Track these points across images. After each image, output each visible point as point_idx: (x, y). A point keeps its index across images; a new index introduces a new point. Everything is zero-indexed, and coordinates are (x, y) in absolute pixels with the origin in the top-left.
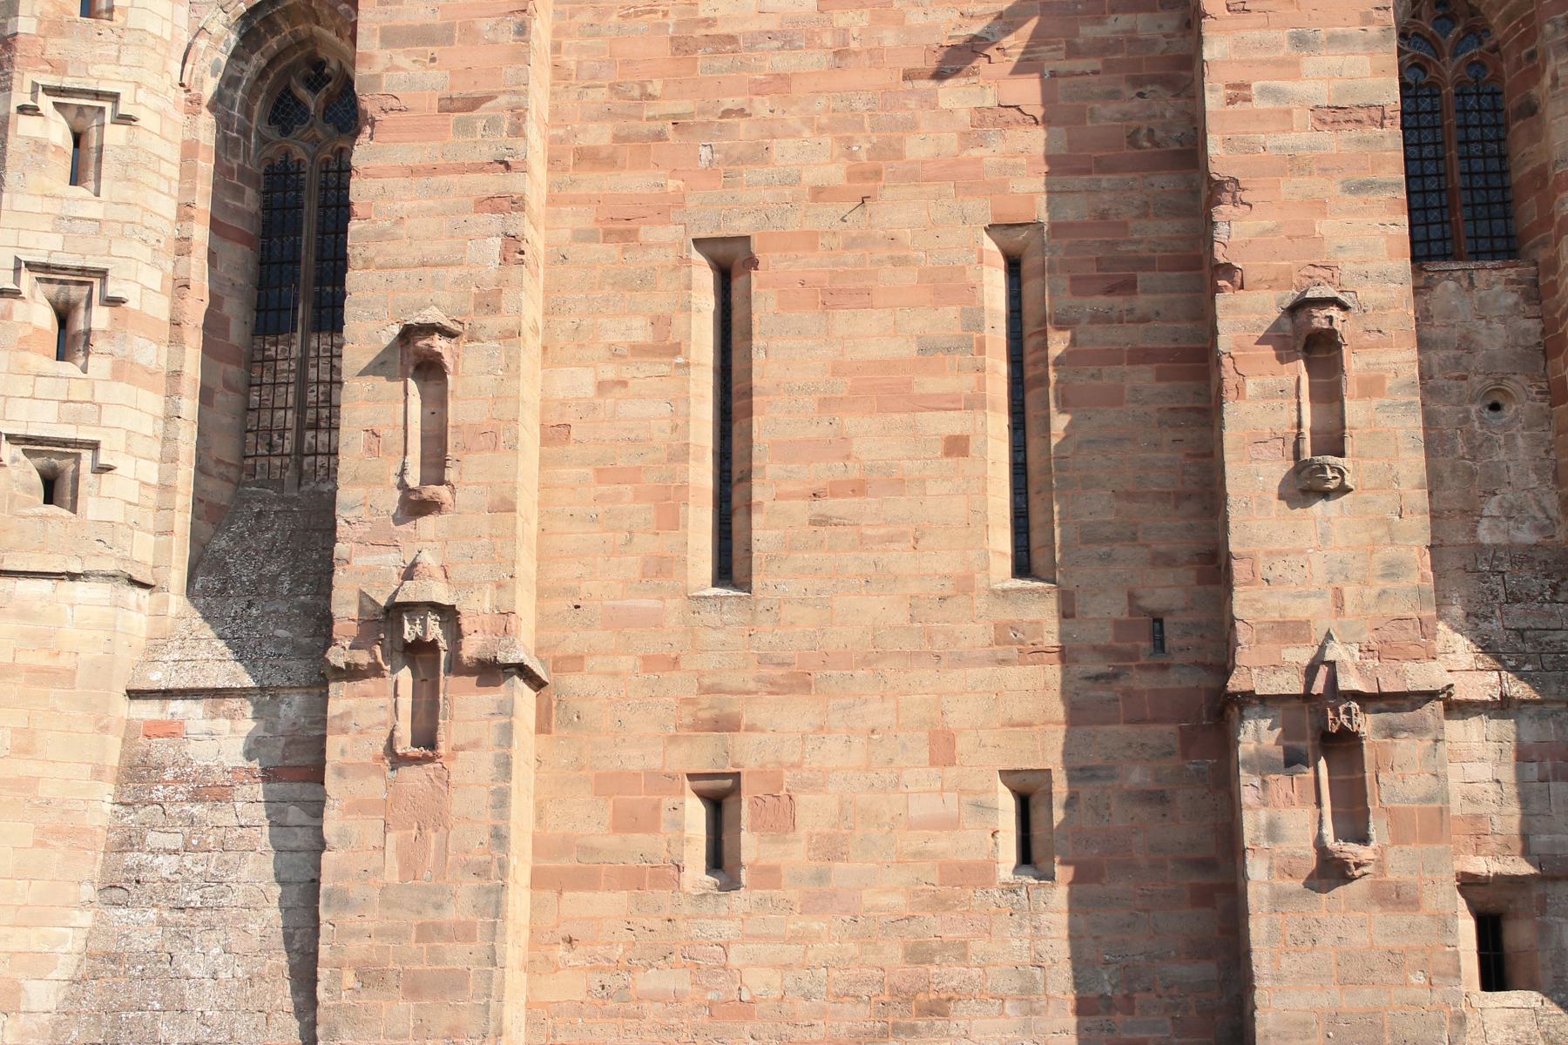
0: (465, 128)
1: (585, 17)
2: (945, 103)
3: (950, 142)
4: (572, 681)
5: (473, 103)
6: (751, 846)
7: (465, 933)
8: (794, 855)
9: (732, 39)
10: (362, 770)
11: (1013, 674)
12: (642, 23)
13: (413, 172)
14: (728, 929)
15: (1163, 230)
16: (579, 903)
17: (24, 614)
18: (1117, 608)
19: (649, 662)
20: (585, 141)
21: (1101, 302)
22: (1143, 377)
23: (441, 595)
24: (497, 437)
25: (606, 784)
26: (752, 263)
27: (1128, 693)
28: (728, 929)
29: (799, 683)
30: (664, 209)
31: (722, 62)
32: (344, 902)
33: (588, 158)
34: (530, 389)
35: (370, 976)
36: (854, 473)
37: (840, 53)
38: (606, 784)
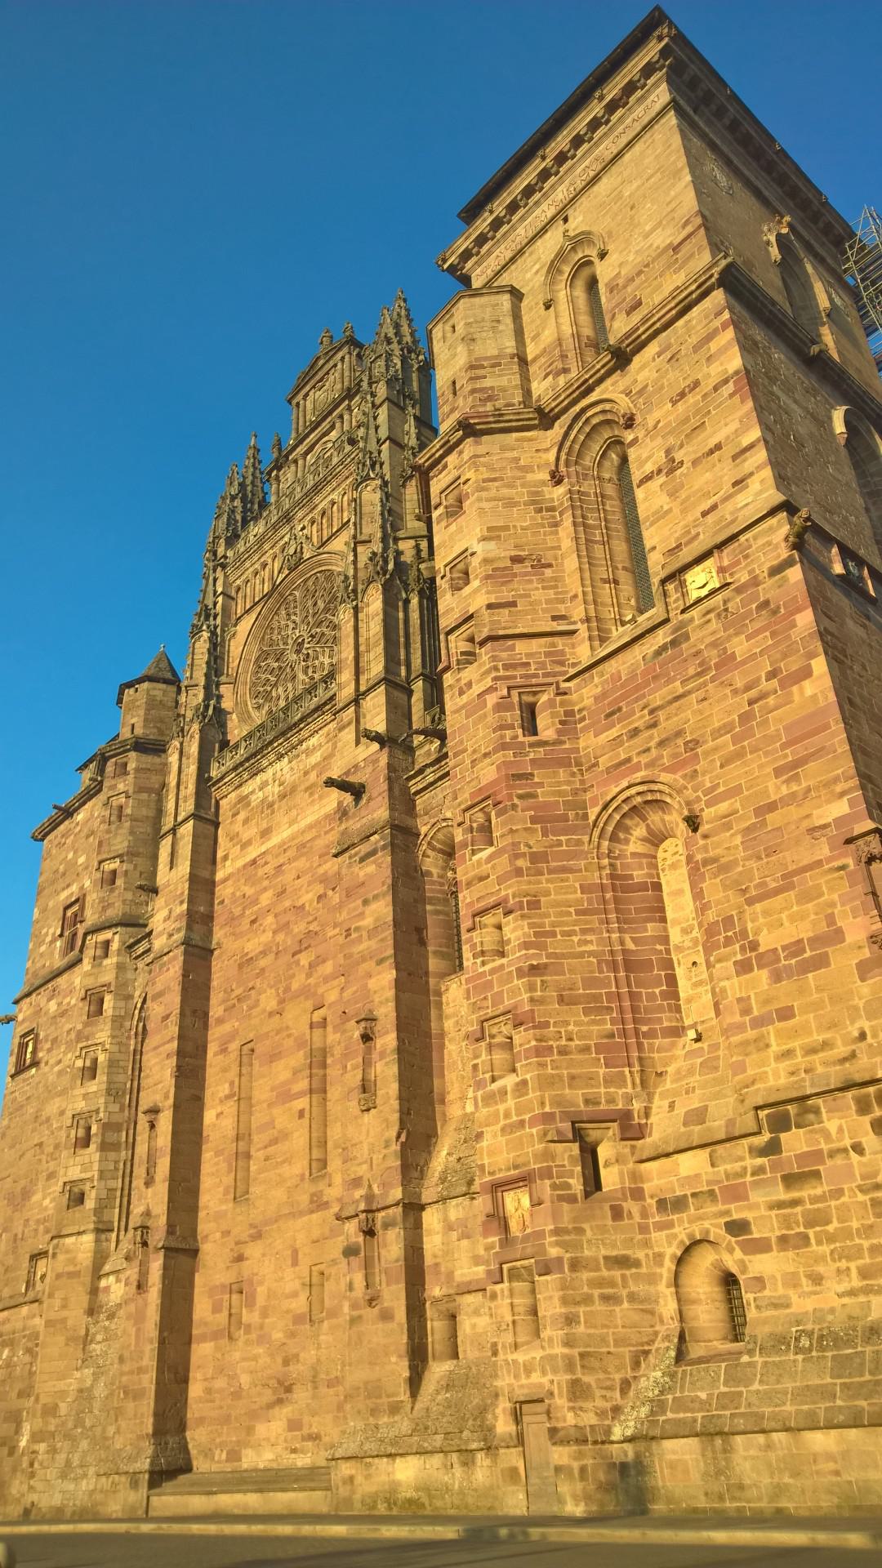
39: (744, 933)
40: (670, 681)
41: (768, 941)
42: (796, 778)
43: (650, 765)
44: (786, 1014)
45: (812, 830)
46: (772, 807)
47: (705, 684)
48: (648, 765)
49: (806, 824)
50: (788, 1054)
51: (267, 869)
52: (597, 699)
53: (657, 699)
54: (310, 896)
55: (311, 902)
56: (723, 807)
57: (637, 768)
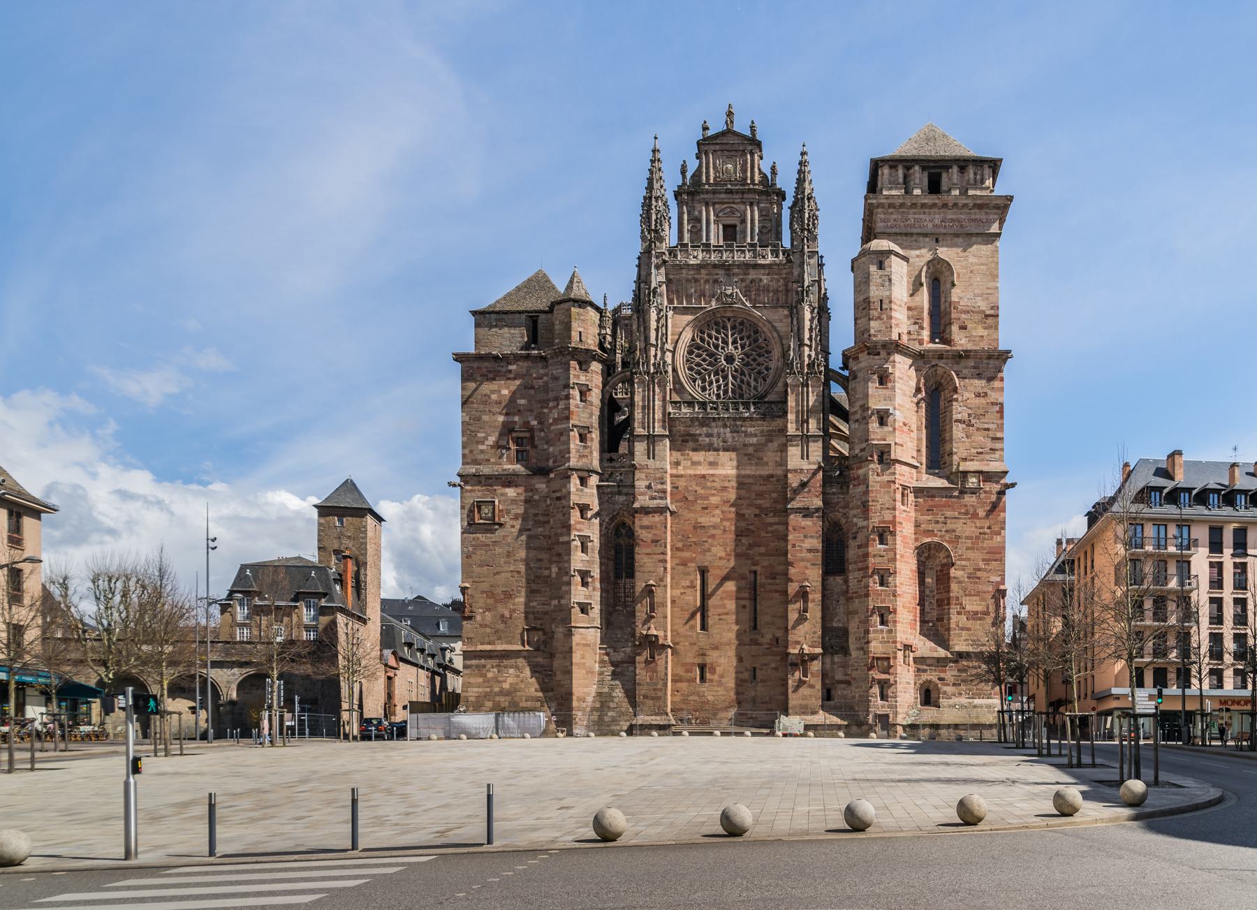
0: (656, 546)
1: (677, 521)
2: (743, 541)
3: (744, 548)
4: (677, 647)
5: (657, 541)
6: (708, 676)
7: (661, 690)
8: (716, 677)
10: (642, 663)
11: (753, 647)
13: (647, 554)
14: (704, 689)
16: (679, 685)
17: (581, 634)
18: (771, 637)
19: (691, 644)
20: (677, 546)
21: (770, 581)
22: (777, 595)
24: (664, 605)
25: (684, 665)
26: (708, 571)
28: (704, 689)
29: (716, 648)
30: (692, 560)
32: (640, 684)
33: (678, 549)
34: (669, 596)
35: (645, 697)
36: (726, 611)
37: (725, 531)
38: (684, 665)
41: (968, 608)
43: (941, 536)
44: (968, 629)
45: (990, 582)
46: (979, 570)
47: (966, 519)
49: (987, 579)
50: (967, 640)
51: (714, 484)
53: (949, 514)
54: (749, 511)
55: (749, 515)
57: (936, 535)
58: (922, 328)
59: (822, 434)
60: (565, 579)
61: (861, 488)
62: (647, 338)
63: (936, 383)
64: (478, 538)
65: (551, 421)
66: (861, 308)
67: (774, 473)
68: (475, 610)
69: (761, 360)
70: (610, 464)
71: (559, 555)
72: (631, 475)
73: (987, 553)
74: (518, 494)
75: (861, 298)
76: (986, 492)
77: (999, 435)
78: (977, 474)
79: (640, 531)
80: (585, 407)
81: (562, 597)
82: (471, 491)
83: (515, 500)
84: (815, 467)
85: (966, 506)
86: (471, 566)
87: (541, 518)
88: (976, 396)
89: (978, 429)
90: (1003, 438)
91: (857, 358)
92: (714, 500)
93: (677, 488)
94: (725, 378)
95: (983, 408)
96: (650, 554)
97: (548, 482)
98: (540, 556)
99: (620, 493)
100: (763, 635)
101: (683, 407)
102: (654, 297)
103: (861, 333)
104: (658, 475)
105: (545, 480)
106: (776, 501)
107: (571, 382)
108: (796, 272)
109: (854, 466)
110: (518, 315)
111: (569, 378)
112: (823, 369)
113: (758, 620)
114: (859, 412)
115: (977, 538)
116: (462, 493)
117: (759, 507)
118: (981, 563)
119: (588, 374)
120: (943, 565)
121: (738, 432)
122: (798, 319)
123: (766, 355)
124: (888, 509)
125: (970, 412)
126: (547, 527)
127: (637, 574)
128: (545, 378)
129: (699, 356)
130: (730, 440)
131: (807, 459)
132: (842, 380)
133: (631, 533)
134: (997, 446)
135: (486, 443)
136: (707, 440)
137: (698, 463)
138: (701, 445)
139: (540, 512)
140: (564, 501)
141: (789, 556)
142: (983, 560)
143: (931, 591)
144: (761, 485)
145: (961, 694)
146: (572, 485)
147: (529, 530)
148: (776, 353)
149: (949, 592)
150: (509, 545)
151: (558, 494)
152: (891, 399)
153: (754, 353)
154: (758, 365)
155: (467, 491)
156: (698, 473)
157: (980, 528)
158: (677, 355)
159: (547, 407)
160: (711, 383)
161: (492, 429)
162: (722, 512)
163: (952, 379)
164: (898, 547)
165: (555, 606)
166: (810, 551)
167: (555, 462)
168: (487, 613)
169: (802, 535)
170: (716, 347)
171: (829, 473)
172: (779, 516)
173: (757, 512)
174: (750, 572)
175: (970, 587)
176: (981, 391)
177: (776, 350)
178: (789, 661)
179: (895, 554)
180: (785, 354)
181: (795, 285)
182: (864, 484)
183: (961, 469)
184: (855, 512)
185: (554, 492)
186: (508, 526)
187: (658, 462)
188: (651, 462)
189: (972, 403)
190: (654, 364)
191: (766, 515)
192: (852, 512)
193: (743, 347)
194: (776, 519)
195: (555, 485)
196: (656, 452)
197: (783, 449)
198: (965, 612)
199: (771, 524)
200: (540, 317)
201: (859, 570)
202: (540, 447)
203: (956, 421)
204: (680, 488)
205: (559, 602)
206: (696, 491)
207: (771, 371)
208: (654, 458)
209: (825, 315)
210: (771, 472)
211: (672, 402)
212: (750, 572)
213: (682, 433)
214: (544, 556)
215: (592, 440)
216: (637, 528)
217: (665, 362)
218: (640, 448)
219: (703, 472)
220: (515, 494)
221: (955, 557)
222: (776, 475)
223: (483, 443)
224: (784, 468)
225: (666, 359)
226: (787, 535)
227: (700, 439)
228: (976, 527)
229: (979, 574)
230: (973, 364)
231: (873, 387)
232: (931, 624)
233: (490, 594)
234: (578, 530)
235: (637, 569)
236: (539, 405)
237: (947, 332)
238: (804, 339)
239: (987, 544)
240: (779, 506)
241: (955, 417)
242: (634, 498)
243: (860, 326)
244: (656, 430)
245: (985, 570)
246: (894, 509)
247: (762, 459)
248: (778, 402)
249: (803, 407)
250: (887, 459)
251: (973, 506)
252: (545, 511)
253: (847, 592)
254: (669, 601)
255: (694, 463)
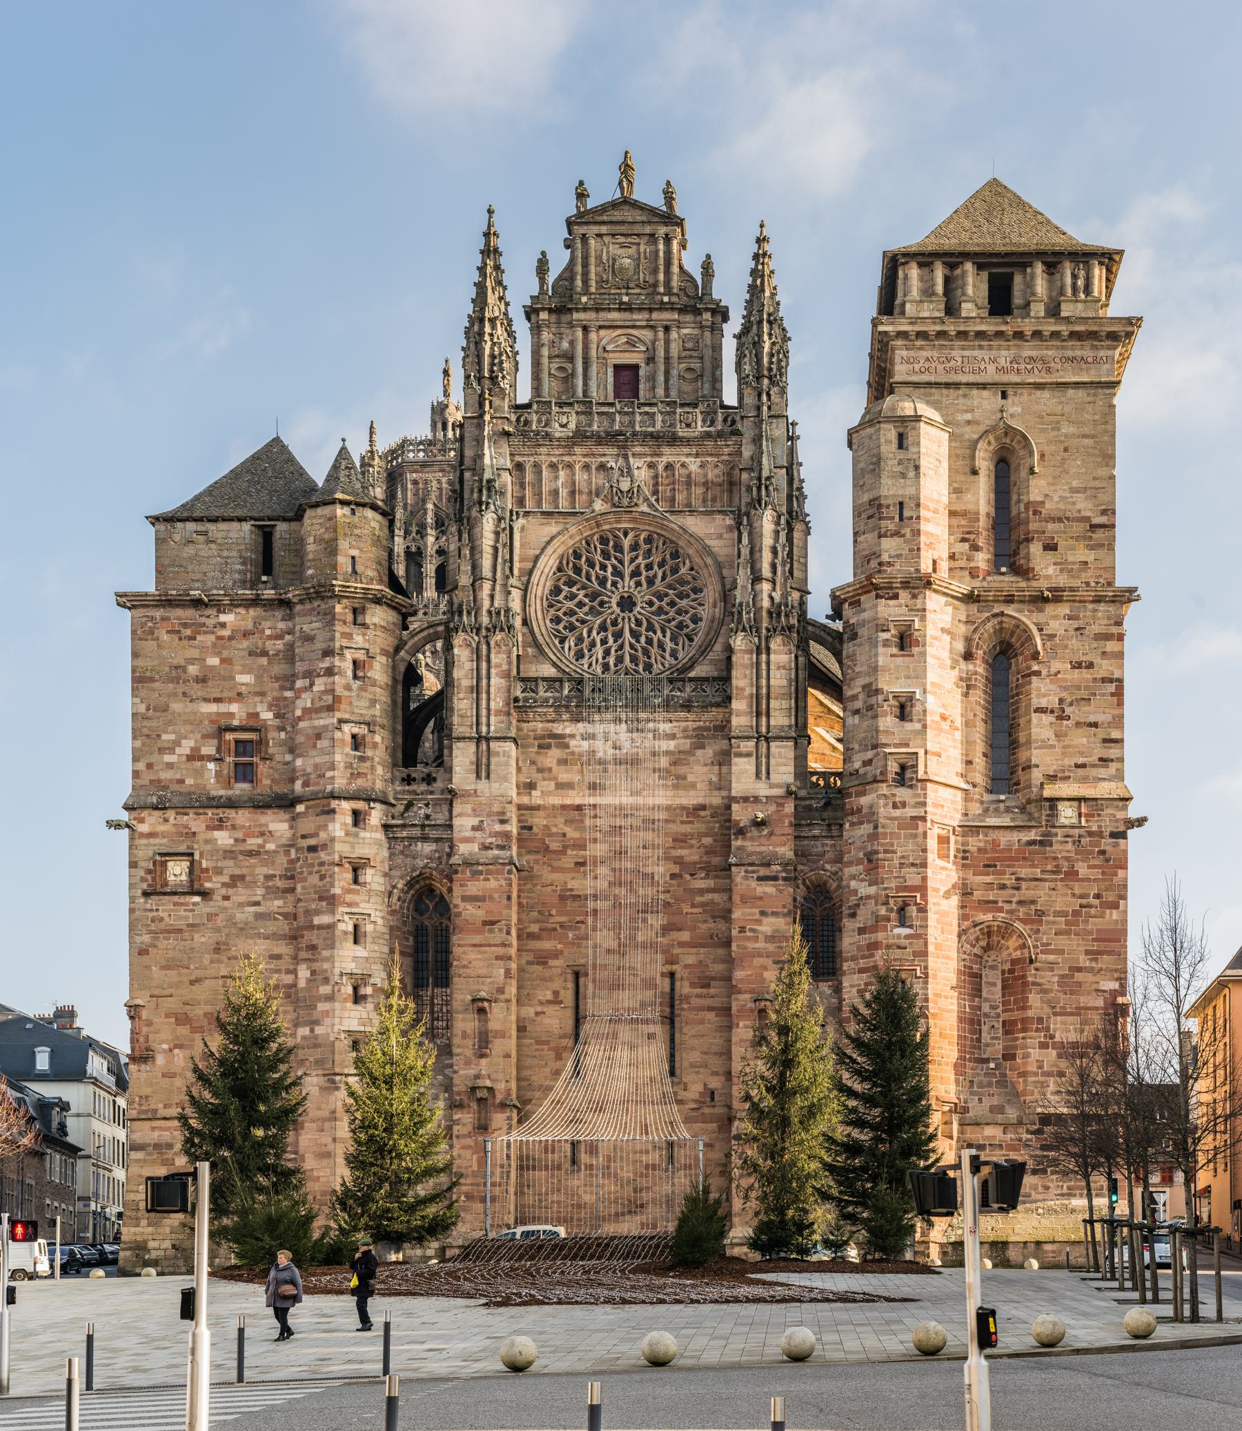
0: (491, 931)
1: (529, 886)
3: (650, 934)
9: (579, 896)
12: (549, 889)
13: (475, 946)
15: (719, 968)
21: (699, 991)
22: (711, 1016)
23: (488, 1083)
27: (703, 1114)
30: (556, 955)
31: (577, 904)
33: (531, 936)
39: (1048, 1029)
40: (1033, 866)
42: (1096, 960)
43: (1008, 912)
45: (1097, 990)
46: (1079, 970)
47: (1056, 880)
48: (1008, 912)
52: (980, 850)
53: (1024, 872)
56: (1051, 958)
57: (1001, 910)
58: (975, 548)
59: (794, 734)
60: (325, 990)
61: (866, 829)
62: (475, 567)
63: (1001, 643)
64: (161, 919)
65: (298, 713)
66: (864, 516)
67: (707, 801)
68: (155, 1046)
69: (684, 603)
70: (407, 788)
71: (312, 948)
72: (445, 807)
73: (1094, 940)
74: (236, 840)
75: (866, 497)
76: (1090, 834)
77: (1115, 734)
78: (1075, 804)
79: (462, 905)
80: (361, 689)
81: (316, 1022)
82: (151, 835)
83: (231, 852)
84: (780, 792)
85: (1055, 858)
86: (148, 967)
87: (280, 883)
88: (1073, 667)
89: (1078, 724)
90: (1122, 740)
91: (859, 602)
92: (599, 850)
93: (530, 828)
94: (618, 635)
95: (1087, 688)
96: (481, 946)
97: (293, 819)
98: (277, 951)
99: (425, 839)
100: (685, 1084)
101: (541, 688)
102: (489, 497)
103: (865, 559)
104: (496, 808)
105: (287, 816)
106: (709, 851)
107: (337, 645)
108: (747, 452)
109: (853, 790)
110: (235, 525)
111: (332, 639)
112: (794, 621)
113: (677, 1059)
114: (861, 696)
115: (1076, 913)
116: (132, 839)
117: (678, 861)
118: (1082, 957)
119: (369, 632)
120: (1014, 962)
121: (642, 731)
122: (750, 534)
123: (693, 596)
124: (913, 865)
125: (1064, 694)
126: (290, 897)
127: (456, 980)
128: (288, 637)
129: (572, 597)
130: (626, 745)
131: (768, 777)
132: (830, 639)
133: (443, 907)
134: (1113, 752)
135: (178, 750)
136: (585, 744)
137: (569, 786)
138: (573, 753)
139: (278, 873)
140: (323, 855)
141: (734, 948)
142: (1087, 952)
143: (992, 1007)
144: (682, 822)
145: (1047, 1188)
146: (338, 826)
147: (257, 904)
148: (711, 592)
149: (1024, 1008)
150: (218, 930)
151: (312, 842)
152: (920, 675)
153: (671, 592)
154: (679, 612)
155: (142, 835)
156: (568, 802)
157: (1081, 897)
158: (531, 597)
159: (292, 688)
160: (593, 644)
161: (188, 728)
162: (614, 870)
163: (1030, 638)
164: (931, 931)
165: (304, 1038)
166: (770, 938)
167: (306, 784)
168: (176, 1051)
169: (757, 911)
170: (602, 582)
171: (807, 802)
172: (717, 877)
173: (676, 870)
174: (663, 975)
175: (1063, 999)
176: (1084, 658)
177: (711, 588)
178: (734, 1132)
179: (926, 944)
180: (726, 595)
181: (745, 476)
182: (869, 822)
183: (1047, 793)
184: (853, 870)
185: (304, 837)
186: (217, 897)
187: (496, 785)
188: (483, 785)
189: (1065, 680)
190: (489, 612)
191: (692, 875)
192: (848, 871)
193: (651, 582)
194: (710, 883)
195: (306, 825)
196: (492, 767)
197: (724, 759)
198: (1054, 1043)
199: (702, 892)
200: (278, 528)
201: (861, 971)
202: (278, 758)
203: (1037, 710)
204: (535, 829)
205: (312, 1031)
206: (564, 835)
207: (702, 624)
208: (488, 777)
209: (798, 527)
210: (701, 800)
211: (523, 680)
212: (663, 975)
213: (539, 732)
214: (283, 949)
215: (375, 745)
216: (456, 900)
217: (508, 610)
218: (462, 757)
219: (578, 801)
220: (232, 841)
221: (1035, 947)
222: (711, 806)
223: (171, 750)
224: (724, 793)
225: (511, 605)
226: (730, 911)
227: (573, 743)
228: (1074, 895)
229: (1079, 976)
230: (1068, 612)
231: (885, 656)
232: (992, 1065)
233: (182, 1019)
234: (350, 905)
235: (453, 971)
236: (276, 685)
237: (1023, 552)
238: (760, 570)
239: (1094, 924)
240: (716, 860)
241: (1036, 702)
242: (451, 847)
243: (865, 545)
244: (492, 728)
245: (1090, 970)
246: (924, 865)
247: (685, 778)
248: (715, 679)
249: (758, 687)
250: (912, 779)
251: (1067, 859)
252: (286, 870)
253: (840, 1009)
254: (514, 1027)
255: (561, 786)
